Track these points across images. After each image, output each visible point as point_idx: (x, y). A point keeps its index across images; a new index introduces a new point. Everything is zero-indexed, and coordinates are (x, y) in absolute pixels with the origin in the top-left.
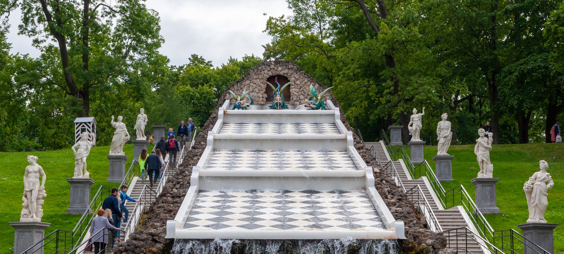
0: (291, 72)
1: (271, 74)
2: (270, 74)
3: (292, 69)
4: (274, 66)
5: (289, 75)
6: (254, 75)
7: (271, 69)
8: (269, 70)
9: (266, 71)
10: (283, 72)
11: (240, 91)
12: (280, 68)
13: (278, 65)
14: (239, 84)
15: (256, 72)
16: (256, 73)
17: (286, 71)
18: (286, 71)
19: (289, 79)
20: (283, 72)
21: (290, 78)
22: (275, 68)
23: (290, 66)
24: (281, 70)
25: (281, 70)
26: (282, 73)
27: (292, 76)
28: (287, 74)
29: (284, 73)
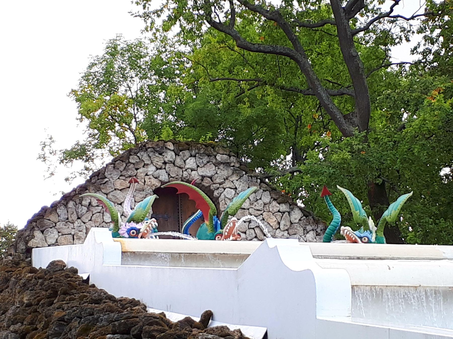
0: (224, 172)
1: (167, 177)
2: (164, 177)
3: (227, 164)
4: (173, 154)
5: (218, 181)
6: (116, 177)
7: (165, 163)
8: (160, 164)
9: (151, 169)
10: (202, 171)
11: (76, 224)
12: (191, 163)
13: (187, 153)
14: (71, 204)
15: (122, 169)
16: (124, 173)
17: (209, 171)
18: (209, 171)
19: (216, 193)
20: (202, 171)
21: (221, 190)
22: (179, 161)
23: (219, 157)
24: (194, 166)
25: (194, 166)
26: (195, 175)
27: (227, 184)
28: (211, 178)
29: (203, 177)
